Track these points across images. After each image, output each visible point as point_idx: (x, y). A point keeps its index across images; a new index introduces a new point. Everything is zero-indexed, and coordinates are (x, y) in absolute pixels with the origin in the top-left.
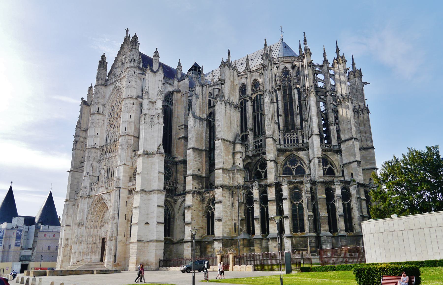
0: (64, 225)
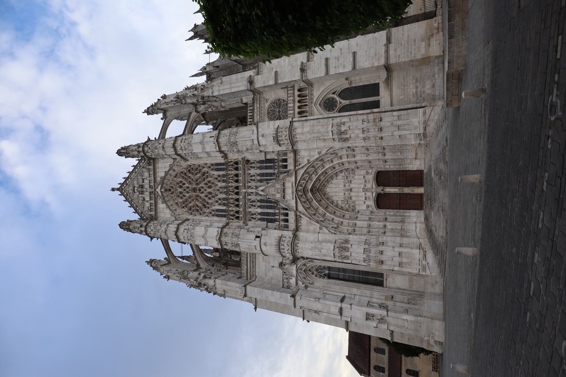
0: (339, 305)
